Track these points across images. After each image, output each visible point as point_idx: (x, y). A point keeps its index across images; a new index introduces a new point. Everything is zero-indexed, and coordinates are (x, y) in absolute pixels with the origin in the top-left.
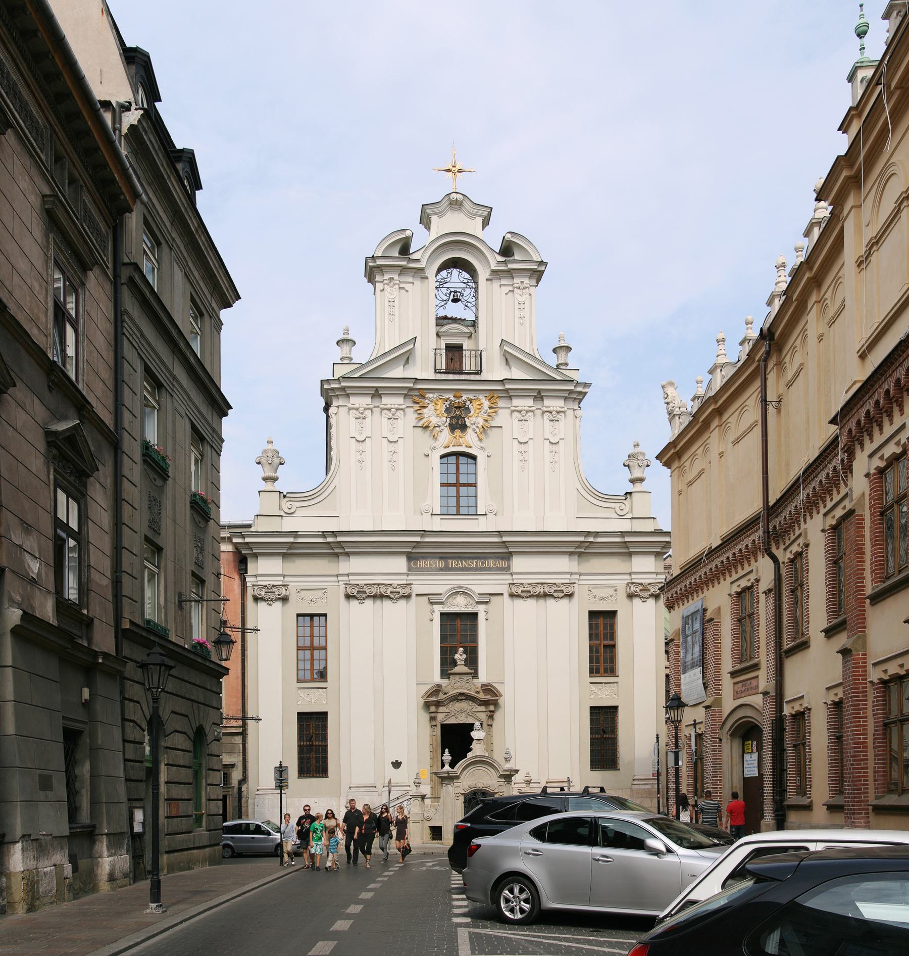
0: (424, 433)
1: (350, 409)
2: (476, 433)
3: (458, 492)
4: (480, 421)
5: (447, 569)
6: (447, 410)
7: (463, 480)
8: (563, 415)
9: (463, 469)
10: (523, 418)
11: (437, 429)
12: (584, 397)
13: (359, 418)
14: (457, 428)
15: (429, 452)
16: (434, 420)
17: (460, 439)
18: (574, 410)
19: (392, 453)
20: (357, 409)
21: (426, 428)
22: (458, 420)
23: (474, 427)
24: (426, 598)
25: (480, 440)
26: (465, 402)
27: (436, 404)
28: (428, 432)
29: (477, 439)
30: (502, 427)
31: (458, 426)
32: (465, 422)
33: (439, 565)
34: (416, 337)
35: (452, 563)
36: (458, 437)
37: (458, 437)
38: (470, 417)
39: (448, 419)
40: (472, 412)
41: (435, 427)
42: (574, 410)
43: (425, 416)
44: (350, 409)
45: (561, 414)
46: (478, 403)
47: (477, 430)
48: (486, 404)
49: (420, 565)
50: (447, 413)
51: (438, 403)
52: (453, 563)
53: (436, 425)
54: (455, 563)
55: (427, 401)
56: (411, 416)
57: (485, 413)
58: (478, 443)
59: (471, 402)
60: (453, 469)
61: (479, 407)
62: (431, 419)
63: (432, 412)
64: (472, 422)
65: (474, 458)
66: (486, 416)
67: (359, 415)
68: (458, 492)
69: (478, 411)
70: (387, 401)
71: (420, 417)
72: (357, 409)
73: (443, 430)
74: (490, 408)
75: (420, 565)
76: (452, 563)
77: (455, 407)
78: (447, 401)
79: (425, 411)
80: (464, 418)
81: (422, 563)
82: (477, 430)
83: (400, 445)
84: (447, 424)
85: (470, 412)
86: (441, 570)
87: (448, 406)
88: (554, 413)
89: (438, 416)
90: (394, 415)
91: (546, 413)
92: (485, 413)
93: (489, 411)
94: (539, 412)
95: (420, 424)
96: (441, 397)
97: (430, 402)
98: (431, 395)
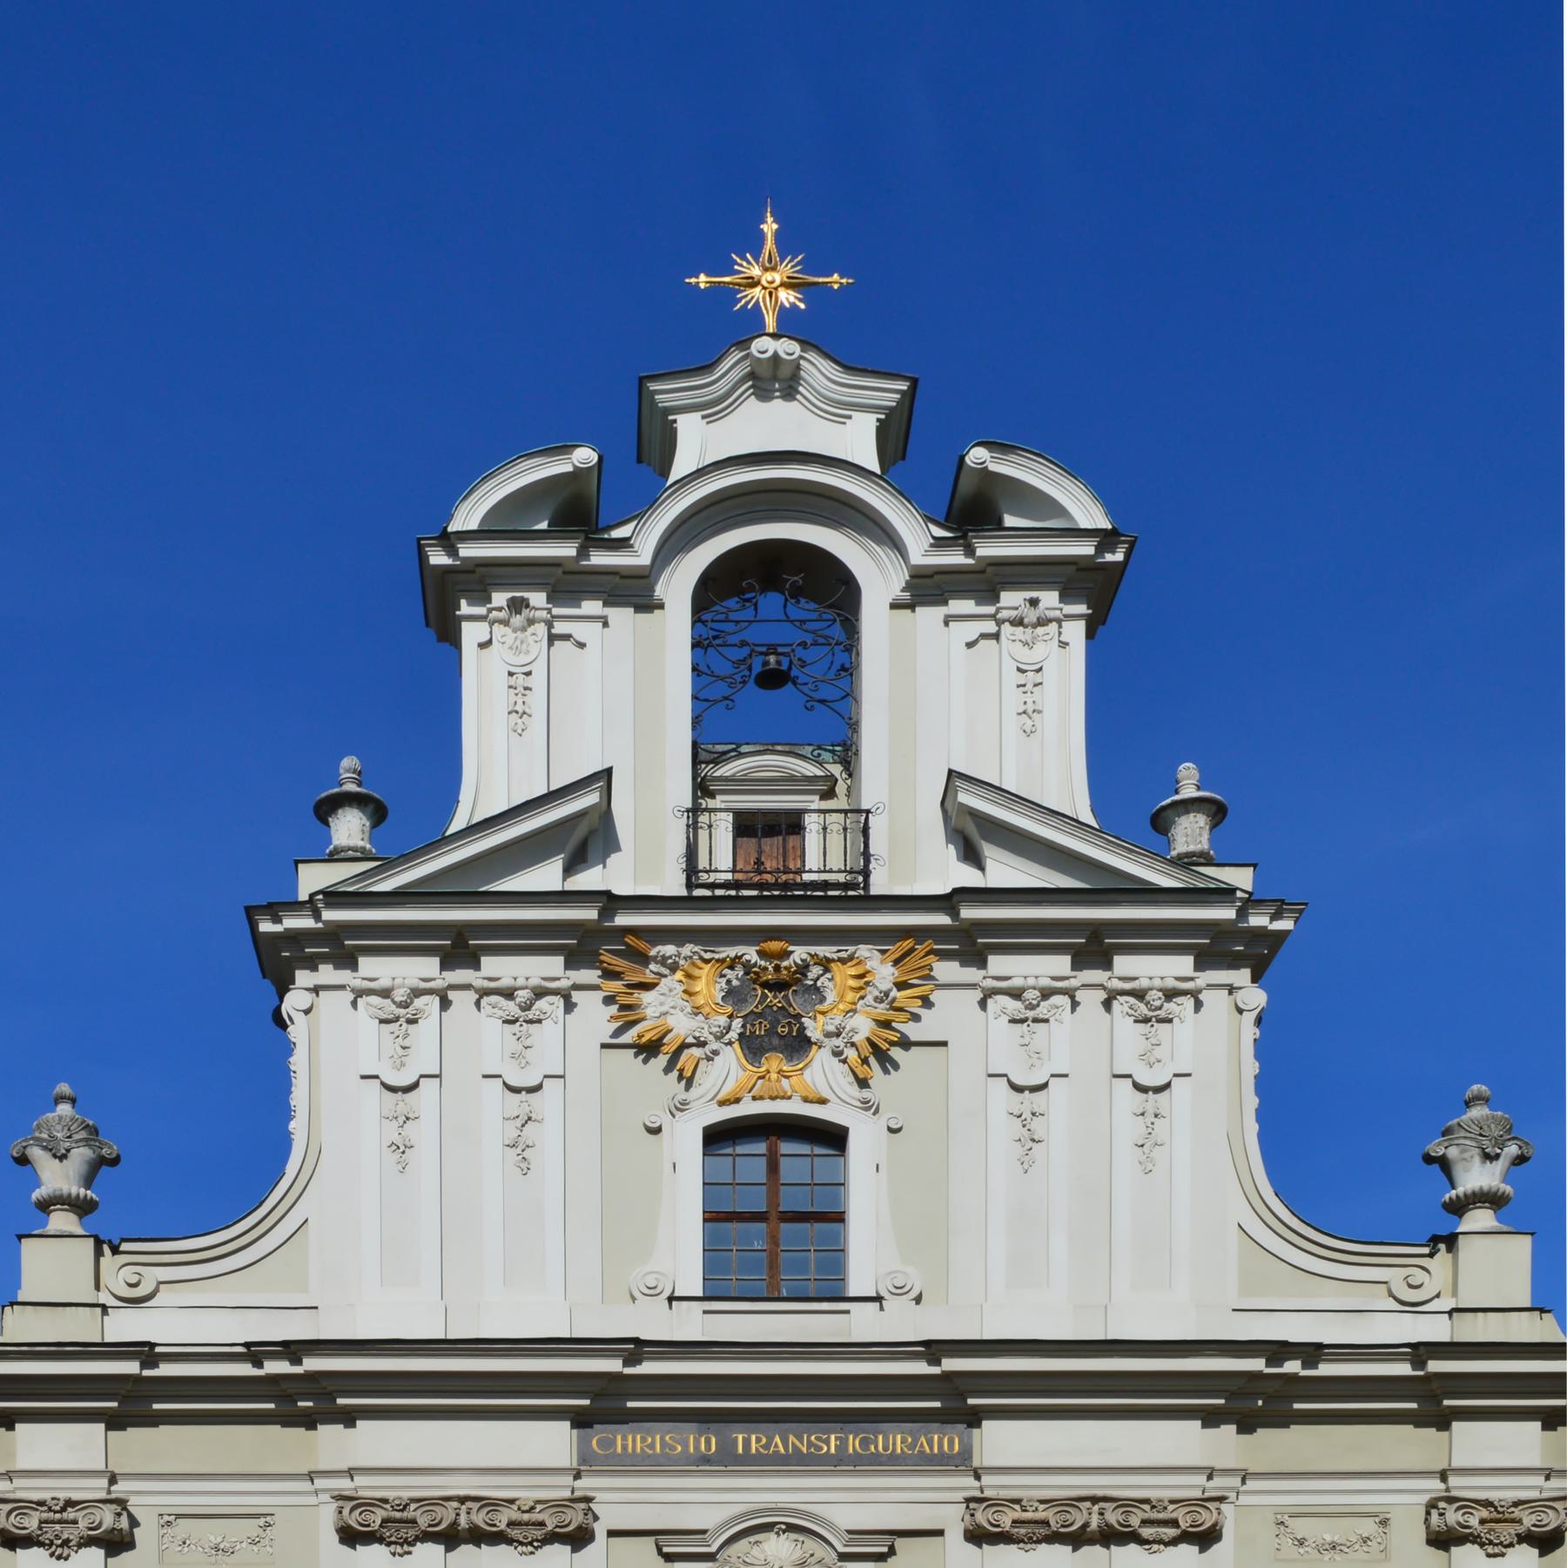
0: (645, 1061)
1: (360, 993)
2: (844, 1061)
3: (774, 1239)
4: (862, 1026)
5: (727, 1460)
6: (731, 994)
7: (790, 1201)
8: (1189, 1002)
9: (791, 1170)
10: (1030, 1014)
11: (696, 1052)
12: (1274, 950)
13: (397, 1019)
14: (774, 1049)
15: (665, 1120)
16: (682, 1025)
17: (785, 1082)
18: (1231, 989)
19: (519, 1123)
20: (385, 993)
21: (648, 1049)
22: (775, 1023)
23: (838, 1042)
24: (652, 1539)
25: (863, 1083)
26: (803, 968)
27: (689, 976)
28: (662, 1060)
29: (851, 1078)
30: (944, 1044)
31: (776, 1041)
32: (802, 1028)
33: (697, 1447)
34: (608, 772)
35: (747, 1443)
36: (774, 1076)
37: (774, 1076)
38: (823, 1013)
39: (737, 1024)
40: (831, 997)
41: (684, 1046)
42: (1231, 989)
43: (649, 1012)
44: (360, 993)
45: (1179, 1000)
46: (853, 972)
47: (851, 1054)
48: (884, 974)
49: (624, 1447)
50: (734, 1004)
51: (696, 972)
52: (747, 1440)
53: (690, 1040)
54: (759, 1440)
55: (653, 967)
56: (594, 1015)
57: (878, 1000)
58: (855, 1091)
59: (827, 970)
60: (755, 1170)
61: (853, 983)
62: (671, 1021)
63: (677, 998)
64: (832, 1028)
65: (834, 1138)
66: (882, 1010)
67: (389, 1008)
68: (774, 1239)
69: (850, 996)
70: (499, 968)
71: (628, 1015)
72: (385, 993)
73: (716, 1053)
74: (901, 986)
75: (624, 1447)
76: (747, 1443)
77: (765, 985)
78: (732, 968)
79: (647, 997)
80: (798, 1017)
81: (629, 1440)
82: (851, 1054)
83: (548, 1103)
84: (733, 1035)
85: (823, 1000)
86: (706, 1460)
87: (735, 983)
88: (1155, 997)
89: (697, 1011)
90: (526, 1007)
91: (1122, 999)
92: (878, 1000)
93: (894, 993)
94: (1091, 1000)
95: (629, 1037)
96: (707, 956)
97: (665, 971)
98: (669, 950)
